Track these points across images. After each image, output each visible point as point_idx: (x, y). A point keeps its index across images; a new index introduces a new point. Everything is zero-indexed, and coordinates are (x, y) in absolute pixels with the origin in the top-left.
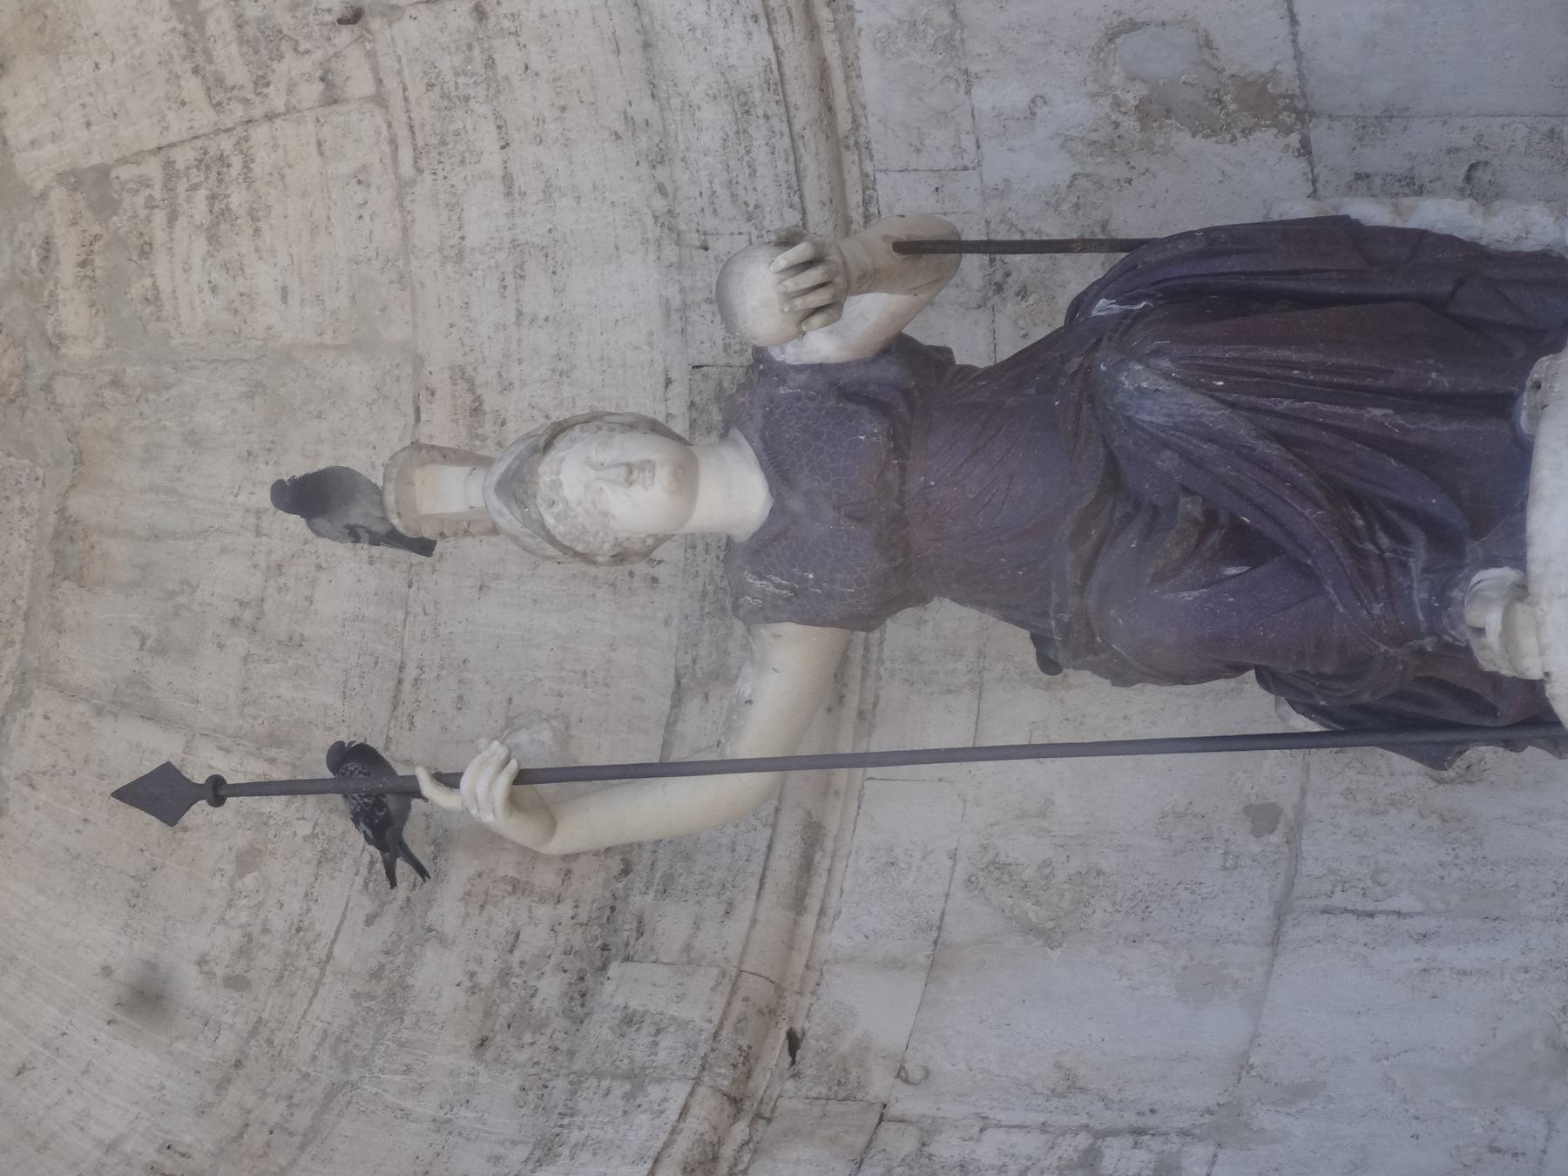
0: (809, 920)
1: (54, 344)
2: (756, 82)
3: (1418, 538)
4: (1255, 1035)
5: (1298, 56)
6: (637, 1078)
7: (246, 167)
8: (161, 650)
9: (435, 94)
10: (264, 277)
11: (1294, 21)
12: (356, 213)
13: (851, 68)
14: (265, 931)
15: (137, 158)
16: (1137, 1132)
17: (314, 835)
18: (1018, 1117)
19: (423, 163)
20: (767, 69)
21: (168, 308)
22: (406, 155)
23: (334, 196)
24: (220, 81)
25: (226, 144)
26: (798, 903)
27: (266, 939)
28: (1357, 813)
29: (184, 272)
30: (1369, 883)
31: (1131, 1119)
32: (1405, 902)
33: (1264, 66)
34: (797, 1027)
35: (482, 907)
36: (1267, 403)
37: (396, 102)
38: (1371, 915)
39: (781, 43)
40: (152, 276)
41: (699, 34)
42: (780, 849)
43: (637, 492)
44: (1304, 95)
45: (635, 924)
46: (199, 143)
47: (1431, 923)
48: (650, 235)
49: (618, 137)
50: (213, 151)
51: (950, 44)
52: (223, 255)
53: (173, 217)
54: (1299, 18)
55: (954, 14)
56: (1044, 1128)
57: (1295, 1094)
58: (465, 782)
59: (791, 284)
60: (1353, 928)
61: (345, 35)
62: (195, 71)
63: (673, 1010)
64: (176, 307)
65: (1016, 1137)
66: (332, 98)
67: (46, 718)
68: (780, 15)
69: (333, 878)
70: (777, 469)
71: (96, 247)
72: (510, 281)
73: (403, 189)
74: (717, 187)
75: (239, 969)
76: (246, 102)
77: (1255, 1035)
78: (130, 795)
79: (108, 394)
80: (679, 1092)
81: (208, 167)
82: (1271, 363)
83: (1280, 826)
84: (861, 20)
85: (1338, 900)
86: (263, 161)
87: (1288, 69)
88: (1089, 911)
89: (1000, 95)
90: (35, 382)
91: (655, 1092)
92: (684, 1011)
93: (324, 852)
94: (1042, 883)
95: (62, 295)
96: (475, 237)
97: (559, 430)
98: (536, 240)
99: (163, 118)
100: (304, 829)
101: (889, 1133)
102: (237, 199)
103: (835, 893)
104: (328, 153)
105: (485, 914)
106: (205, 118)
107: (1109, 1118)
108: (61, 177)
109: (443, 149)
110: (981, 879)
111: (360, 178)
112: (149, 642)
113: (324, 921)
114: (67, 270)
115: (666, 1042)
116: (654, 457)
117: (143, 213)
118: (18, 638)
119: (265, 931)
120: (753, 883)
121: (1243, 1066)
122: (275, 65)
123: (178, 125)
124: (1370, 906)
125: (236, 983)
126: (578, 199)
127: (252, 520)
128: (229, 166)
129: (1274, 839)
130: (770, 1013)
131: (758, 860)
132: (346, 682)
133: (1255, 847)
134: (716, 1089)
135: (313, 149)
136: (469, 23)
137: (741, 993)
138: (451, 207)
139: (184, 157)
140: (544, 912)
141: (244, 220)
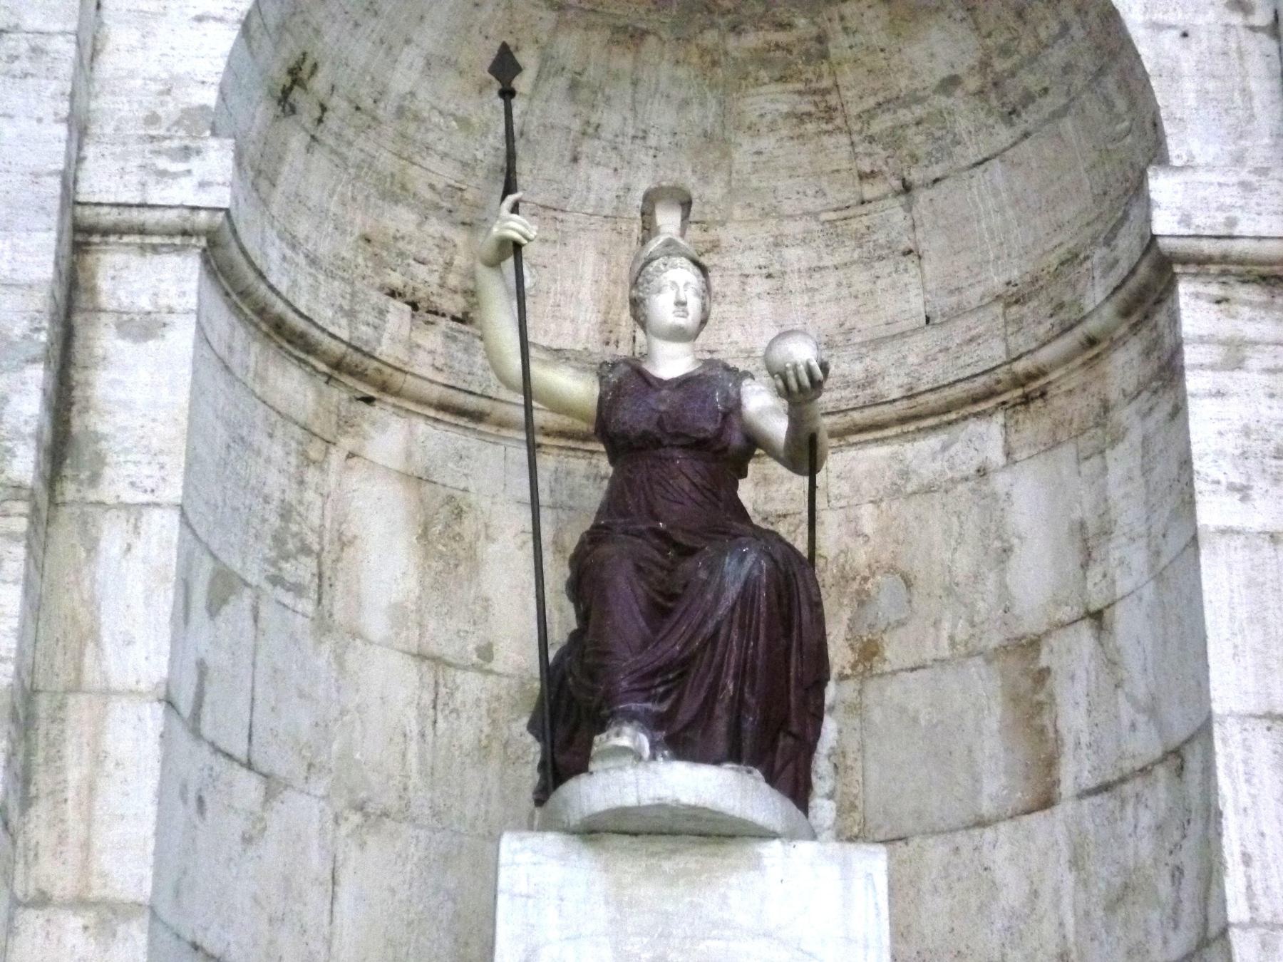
0: (432, 413)
1: (736, 29)
2: (876, 391)
3: (664, 707)
4: (371, 643)
5: (894, 673)
6: (351, 314)
7: (826, 132)
9: (864, 230)
10: (767, 143)
11: (913, 670)
13: (883, 440)
14: (427, 130)
16: (320, 576)
17: (476, 160)
18: (328, 513)
19: (827, 225)
20: (883, 396)
21: (752, 91)
22: (833, 216)
24: (872, 117)
26: (443, 407)
27: (423, 130)
29: (771, 100)
30: (451, 706)
31: (327, 573)
32: (441, 724)
33: (888, 654)
34: (376, 403)
36: (735, 625)
37: (862, 210)
38: (434, 707)
43: (673, 308)
44: (872, 676)
46: (839, 107)
47: (430, 738)
49: (841, 325)
51: (896, 492)
52: (780, 121)
53: (800, 93)
55: (914, 493)
56: (322, 526)
57: (340, 660)
58: (514, 216)
59: (802, 368)
60: (427, 698)
61: (897, 184)
63: (386, 335)
65: (317, 513)
66: (863, 177)
68: (913, 402)
70: (684, 383)
72: (764, 271)
73: (815, 215)
75: (408, 114)
76: (860, 132)
77: (371, 643)
79: (708, 59)
80: (345, 335)
82: (757, 629)
84: (908, 446)
85: (443, 690)
86: (828, 141)
87: (887, 668)
89: (868, 519)
91: (344, 322)
92: (385, 340)
95: (761, 34)
97: (703, 270)
100: (480, 155)
101: (319, 444)
102: (811, 127)
106: (854, 110)
107: (327, 559)
113: (433, 162)
115: (370, 331)
116: (690, 318)
120: (452, 383)
121: (356, 634)
123: (849, 95)
124: (439, 707)
125: (401, 112)
126: (808, 305)
127: (641, 134)
130: (384, 388)
131: (464, 386)
133: (471, 647)
134: (344, 356)
135: (835, 168)
136: (902, 248)
139: (833, 100)
140: (434, 279)
141: (797, 131)
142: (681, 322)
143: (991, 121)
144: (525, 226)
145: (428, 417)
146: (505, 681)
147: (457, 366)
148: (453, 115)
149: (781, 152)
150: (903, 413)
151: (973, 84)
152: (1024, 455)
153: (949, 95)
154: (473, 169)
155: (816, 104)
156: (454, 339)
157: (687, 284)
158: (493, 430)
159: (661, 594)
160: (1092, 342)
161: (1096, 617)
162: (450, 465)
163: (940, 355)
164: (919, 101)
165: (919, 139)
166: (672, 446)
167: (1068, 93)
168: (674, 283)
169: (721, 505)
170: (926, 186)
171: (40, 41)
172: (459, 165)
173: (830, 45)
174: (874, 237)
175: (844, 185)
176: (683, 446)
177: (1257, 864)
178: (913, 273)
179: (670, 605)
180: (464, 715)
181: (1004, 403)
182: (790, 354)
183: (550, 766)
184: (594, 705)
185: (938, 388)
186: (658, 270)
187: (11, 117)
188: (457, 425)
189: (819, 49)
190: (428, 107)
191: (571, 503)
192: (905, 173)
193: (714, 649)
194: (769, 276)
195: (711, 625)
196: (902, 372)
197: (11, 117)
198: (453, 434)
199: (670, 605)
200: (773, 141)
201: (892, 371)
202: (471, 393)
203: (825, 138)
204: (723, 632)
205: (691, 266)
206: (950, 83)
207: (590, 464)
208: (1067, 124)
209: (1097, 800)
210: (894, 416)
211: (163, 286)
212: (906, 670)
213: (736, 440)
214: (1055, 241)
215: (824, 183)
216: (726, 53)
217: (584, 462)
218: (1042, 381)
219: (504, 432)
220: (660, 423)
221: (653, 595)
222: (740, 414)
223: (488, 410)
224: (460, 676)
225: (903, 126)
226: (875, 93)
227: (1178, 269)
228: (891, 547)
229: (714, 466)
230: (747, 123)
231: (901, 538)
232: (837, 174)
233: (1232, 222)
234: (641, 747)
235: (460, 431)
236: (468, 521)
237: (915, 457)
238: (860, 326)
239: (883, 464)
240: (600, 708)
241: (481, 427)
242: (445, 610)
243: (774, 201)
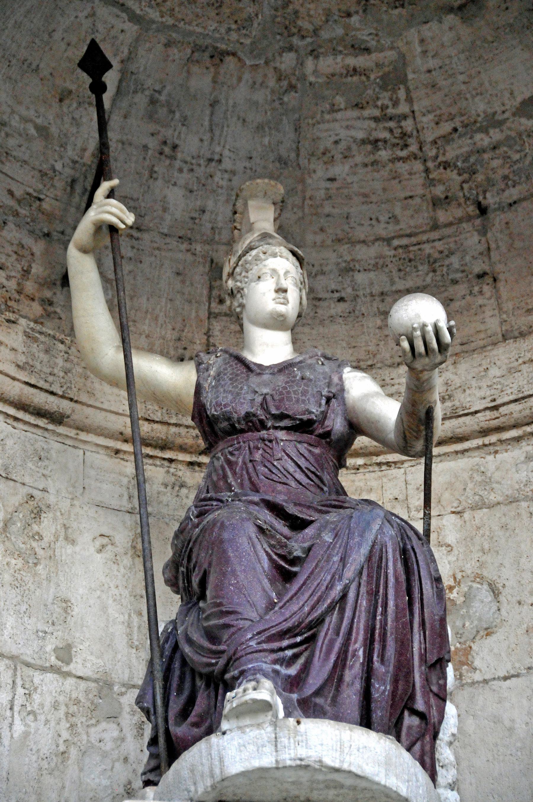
1: (314, 53)
2: (457, 404)
3: (293, 671)
7: (400, 159)
8: (153, 102)
10: (340, 170)
11: (505, 678)
12: (373, 217)
14: (7, 135)
15: (409, 100)
17: (55, 171)
19: (400, 251)
20: (464, 408)
22: (405, 241)
23: (383, 206)
25: (414, 148)
28: (67, 705)
30: (29, 709)
33: (477, 663)
35: (16, 253)
36: (363, 589)
37: (435, 235)
38: (11, 709)
39: (479, 415)
40: (346, 109)
41: (483, 374)
42: (51, 398)
43: (274, 295)
45: (13, 319)
46: (415, 133)
48: (362, 363)
50: (410, 141)
52: (354, 147)
53: (376, 119)
54: (508, 681)
59: (430, 328)
62: (455, 130)
64: (328, 121)
66: (436, 203)
67: (122, 31)
68: (496, 414)
69: (33, 177)
70: (284, 368)
71: (364, 78)
72: (337, 295)
73: (388, 241)
74: (396, 387)
78: (93, 46)
79: (285, 83)
81: (401, 138)
82: (386, 595)
83: (60, 663)
84: (490, 458)
85: (20, 691)
86: (403, 168)
87: (477, 677)
88: (16, 556)
90: (295, 40)
93: (46, 174)
94: (31, 534)
95: (339, 58)
96: (361, 278)
98: (358, 308)
99: (429, 112)
100: (58, 166)
102: (384, 154)
103: (26, 428)
104: (406, 201)
105: (12, 254)
106: (429, 136)
108: (402, 56)
109: (407, 260)
110: (32, 503)
111: (394, 219)
112: (157, 95)
114: (352, 61)
117: (379, 103)
118: (164, 20)
119: (7, 135)
120: (33, 382)
122: (455, 171)
123: (427, 120)
124: (16, 708)
126: (380, 328)
127: (217, 157)
128: (402, 150)
129: (53, 658)
131: (46, 386)
132: (132, 199)
133: (49, 648)
135: (409, 194)
138: (376, 265)
140: (12, 285)
141: (372, 158)
142: (282, 309)
144: (121, 210)
145: (7, 415)
146: (83, 685)
147: (38, 366)
148: (31, 121)
149: (355, 179)
150: (484, 425)
154: (52, 179)
155: (391, 131)
156: (36, 340)
157: (287, 273)
158: (72, 433)
159: (283, 557)
162: (30, 465)
164: (499, 124)
165: (495, 163)
166: (276, 428)
168: (274, 271)
169: (325, 489)
170: (501, 208)
172: (36, 173)
173: (409, 71)
175: (417, 211)
178: (488, 295)
179: (295, 569)
180: (42, 718)
182: (418, 316)
183: (161, 740)
184: (217, 669)
185: (523, 398)
186: (257, 259)
188: (36, 426)
190: (9, 110)
192: (481, 198)
193: (342, 611)
194: (341, 300)
195: (339, 587)
196: (484, 384)
198: (33, 435)
199: (295, 569)
200: (347, 167)
201: (474, 383)
202: (52, 393)
203: (399, 165)
204: (351, 595)
205: (290, 256)
207: (168, 472)
210: (477, 428)
212: (499, 679)
213: (337, 424)
216: (303, 78)
217: (162, 470)
219: (83, 436)
220: (264, 405)
221: (275, 557)
222: (343, 402)
223: (68, 412)
224: (37, 677)
225: (481, 151)
226: (451, 118)
228: (476, 555)
229: (317, 451)
230: (322, 149)
231: (486, 546)
232: (410, 201)
234: (276, 704)
235: (39, 432)
236: (47, 519)
237: (497, 469)
239: (466, 476)
240: (225, 670)
241: (61, 429)
242: (24, 608)
243: (346, 227)
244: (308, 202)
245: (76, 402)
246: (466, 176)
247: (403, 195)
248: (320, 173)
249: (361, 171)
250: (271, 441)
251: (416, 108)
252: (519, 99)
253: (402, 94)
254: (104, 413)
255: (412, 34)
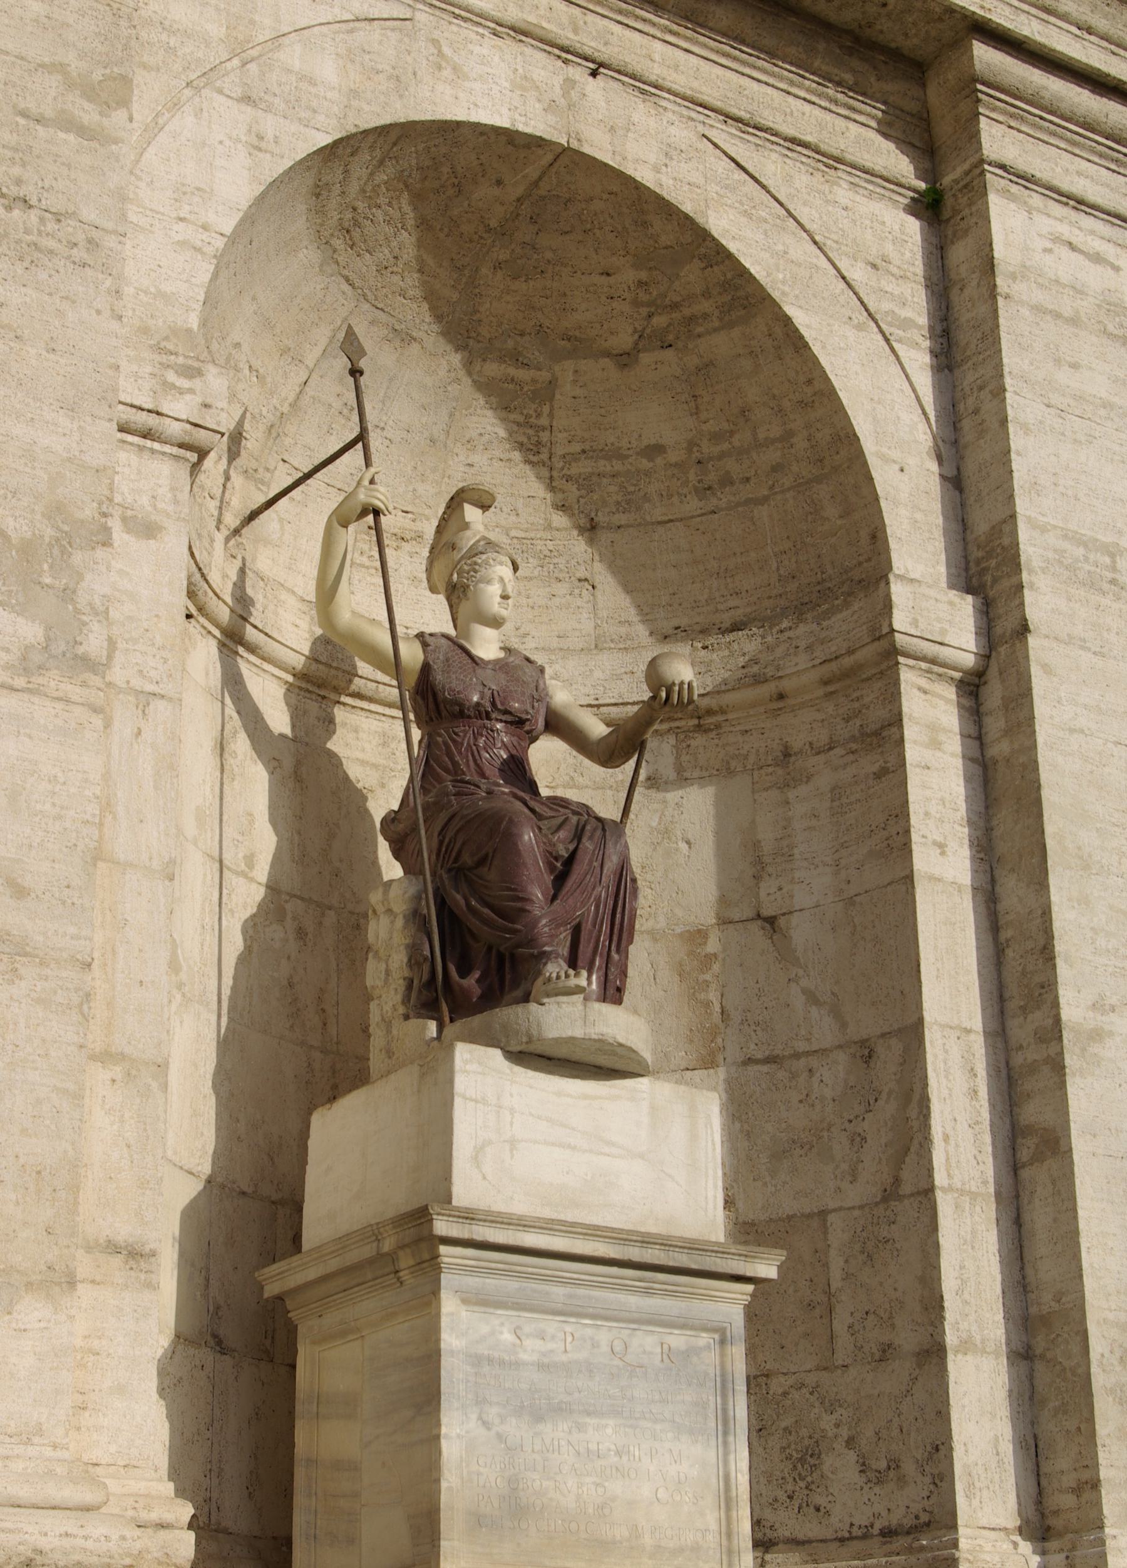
15: (551, 415)
19: (515, 541)
24: (576, 460)
25: (544, 456)
43: (498, 599)
50: (543, 449)
53: (518, 424)
62: (584, 451)
71: (518, 387)
76: (562, 469)
90: (471, 342)
100: (264, 413)
106: (559, 450)
117: (525, 412)
123: (562, 437)
133: (240, 855)
137: (215, 598)
139: (545, 436)
143: (685, 491)
151: (673, 457)
152: (696, 774)
153: (651, 460)
155: (529, 438)
160: (781, 696)
161: (771, 921)
163: (625, 676)
164: (623, 458)
165: (613, 489)
166: (497, 720)
167: (772, 487)
168: (502, 580)
170: (609, 527)
171: (95, 234)
174: (555, 561)
176: (506, 722)
177: (952, 1143)
181: (678, 728)
187: (74, 302)
189: (546, 393)
191: (307, 740)
197: (74, 302)
206: (655, 450)
208: (762, 513)
209: (765, 1068)
211: (160, 491)
214: (731, 604)
215: (520, 504)
218: (720, 718)
219: (266, 666)
227: (901, 659)
233: (943, 632)
238: (533, 633)
244: (446, 479)
245: (269, 636)
246: (583, 492)
247: (526, 495)
248: (462, 458)
249: (497, 464)
250: (492, 731)
251: (554, 424)
252: (645, 443)
253: (546, 409)
254: (364, 681)
255: (569, 365)
